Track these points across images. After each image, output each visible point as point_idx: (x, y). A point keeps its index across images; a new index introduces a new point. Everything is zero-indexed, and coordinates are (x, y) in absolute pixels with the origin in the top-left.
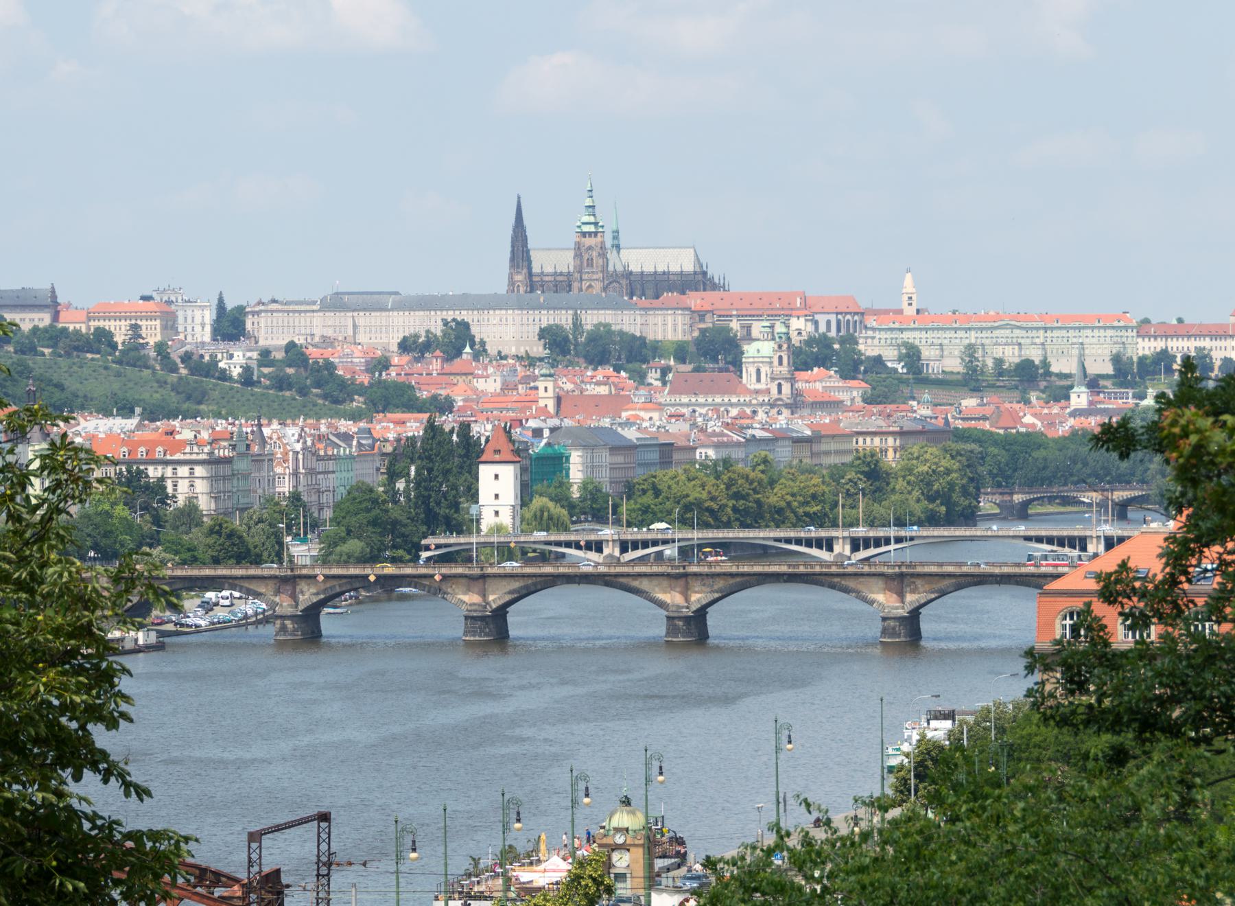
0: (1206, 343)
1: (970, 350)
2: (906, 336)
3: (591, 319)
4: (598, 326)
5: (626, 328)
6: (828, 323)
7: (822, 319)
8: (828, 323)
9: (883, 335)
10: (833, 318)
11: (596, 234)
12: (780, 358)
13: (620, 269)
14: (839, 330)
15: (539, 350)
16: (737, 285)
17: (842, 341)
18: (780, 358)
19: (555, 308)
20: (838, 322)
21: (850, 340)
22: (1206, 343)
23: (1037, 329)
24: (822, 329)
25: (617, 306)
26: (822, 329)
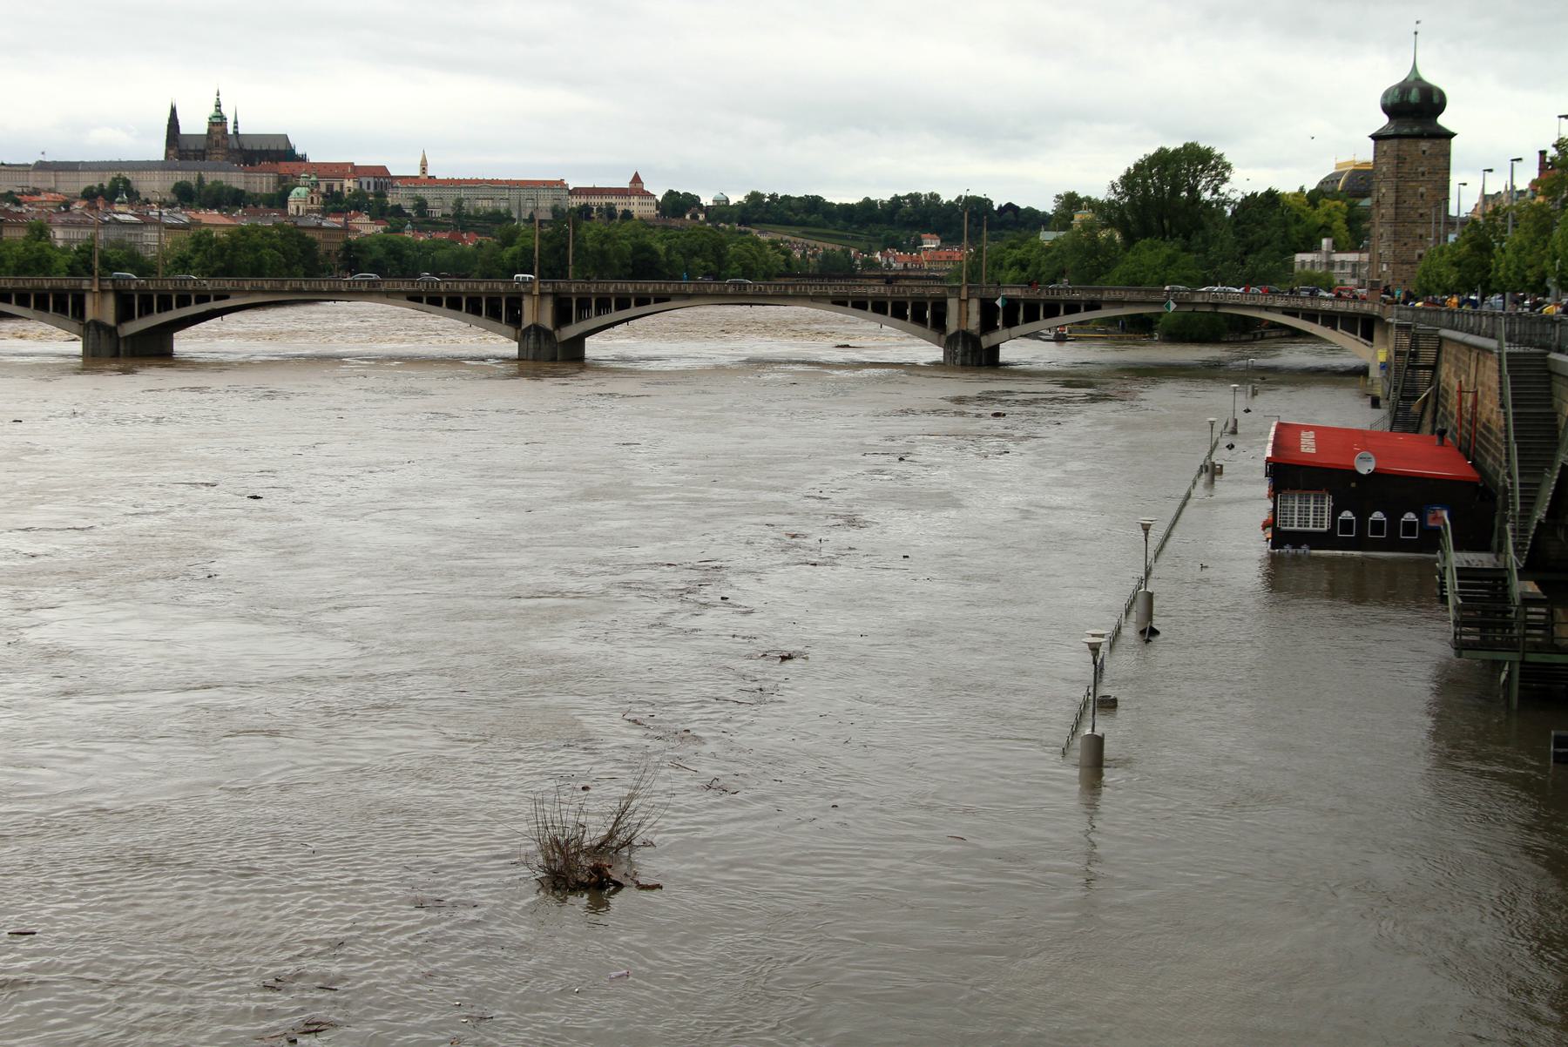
0: (613, 200)
1: (459, 203)
2: (419, 192)
3: (210, 178)
4: (215, 183)
5: (235, 185)
6: (369, 183)
7: (364, 181)
8: (369, 183)
9: (404, 192)
10: (372, 180)
11: (221, 124)
12: (312, 198)
13: (236, 147)
14: (375, 188)
15: (174, 198)
16: (312, 159)
17: (376, 195)
18: (312, 198)
19: (186, 170)
20: (376, 183)
21: (381, 195)
22: (613, 200)
23: (505, 188)
24: (365, 186)
25: (228, 170)
26: (365, 186)
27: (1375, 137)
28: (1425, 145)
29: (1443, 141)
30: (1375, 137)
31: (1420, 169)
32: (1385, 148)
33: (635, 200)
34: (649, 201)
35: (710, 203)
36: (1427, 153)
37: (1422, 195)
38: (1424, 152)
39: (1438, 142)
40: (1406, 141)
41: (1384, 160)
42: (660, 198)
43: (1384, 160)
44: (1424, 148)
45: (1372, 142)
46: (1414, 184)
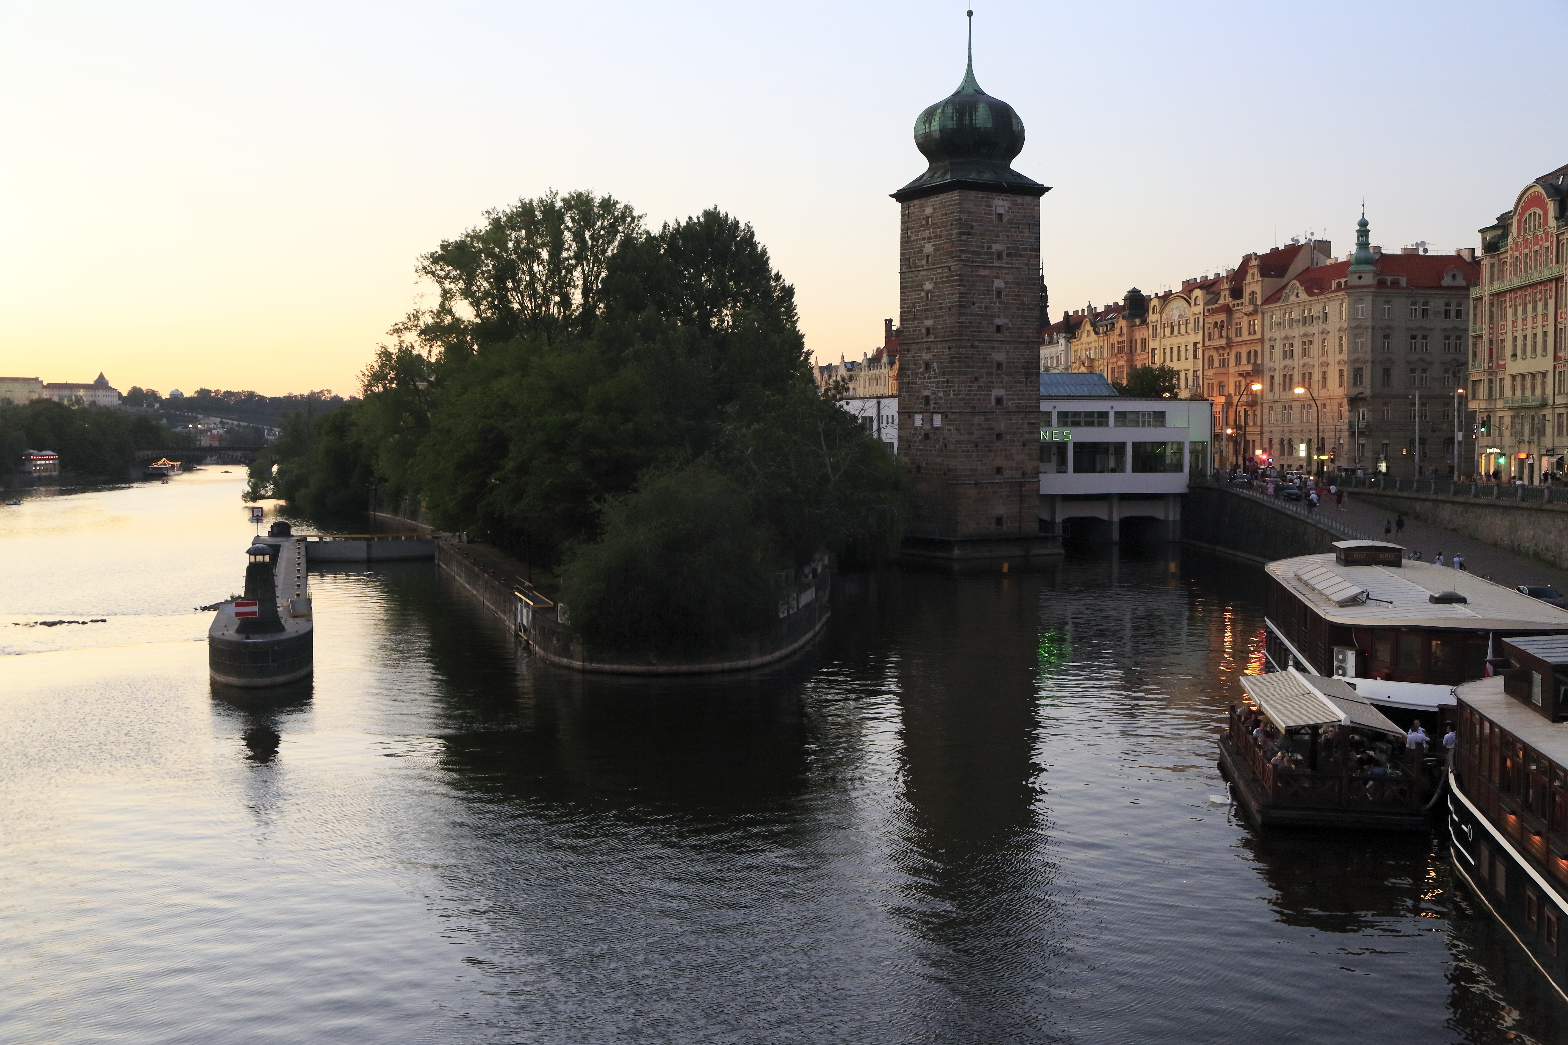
27: (902, 196)
28: (1001, 204)
29: (1028, 199)
30: (902, 196)
31: (996, 247)
32: (928, 211)
33: (100, 393)
34: (112, 394)
35: (168, 397)
36: (1005, 219)
37: (999, 294)
38: (1000, 215)
39: (1019, 200)
40: (972, 194)
41: (926, 234)
42: (125, 394)
43: (926, 234)
44: (1001, 211)
45: (896, 207)
46: (986, 272)
